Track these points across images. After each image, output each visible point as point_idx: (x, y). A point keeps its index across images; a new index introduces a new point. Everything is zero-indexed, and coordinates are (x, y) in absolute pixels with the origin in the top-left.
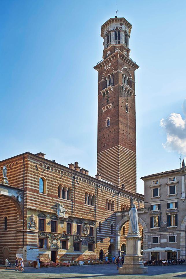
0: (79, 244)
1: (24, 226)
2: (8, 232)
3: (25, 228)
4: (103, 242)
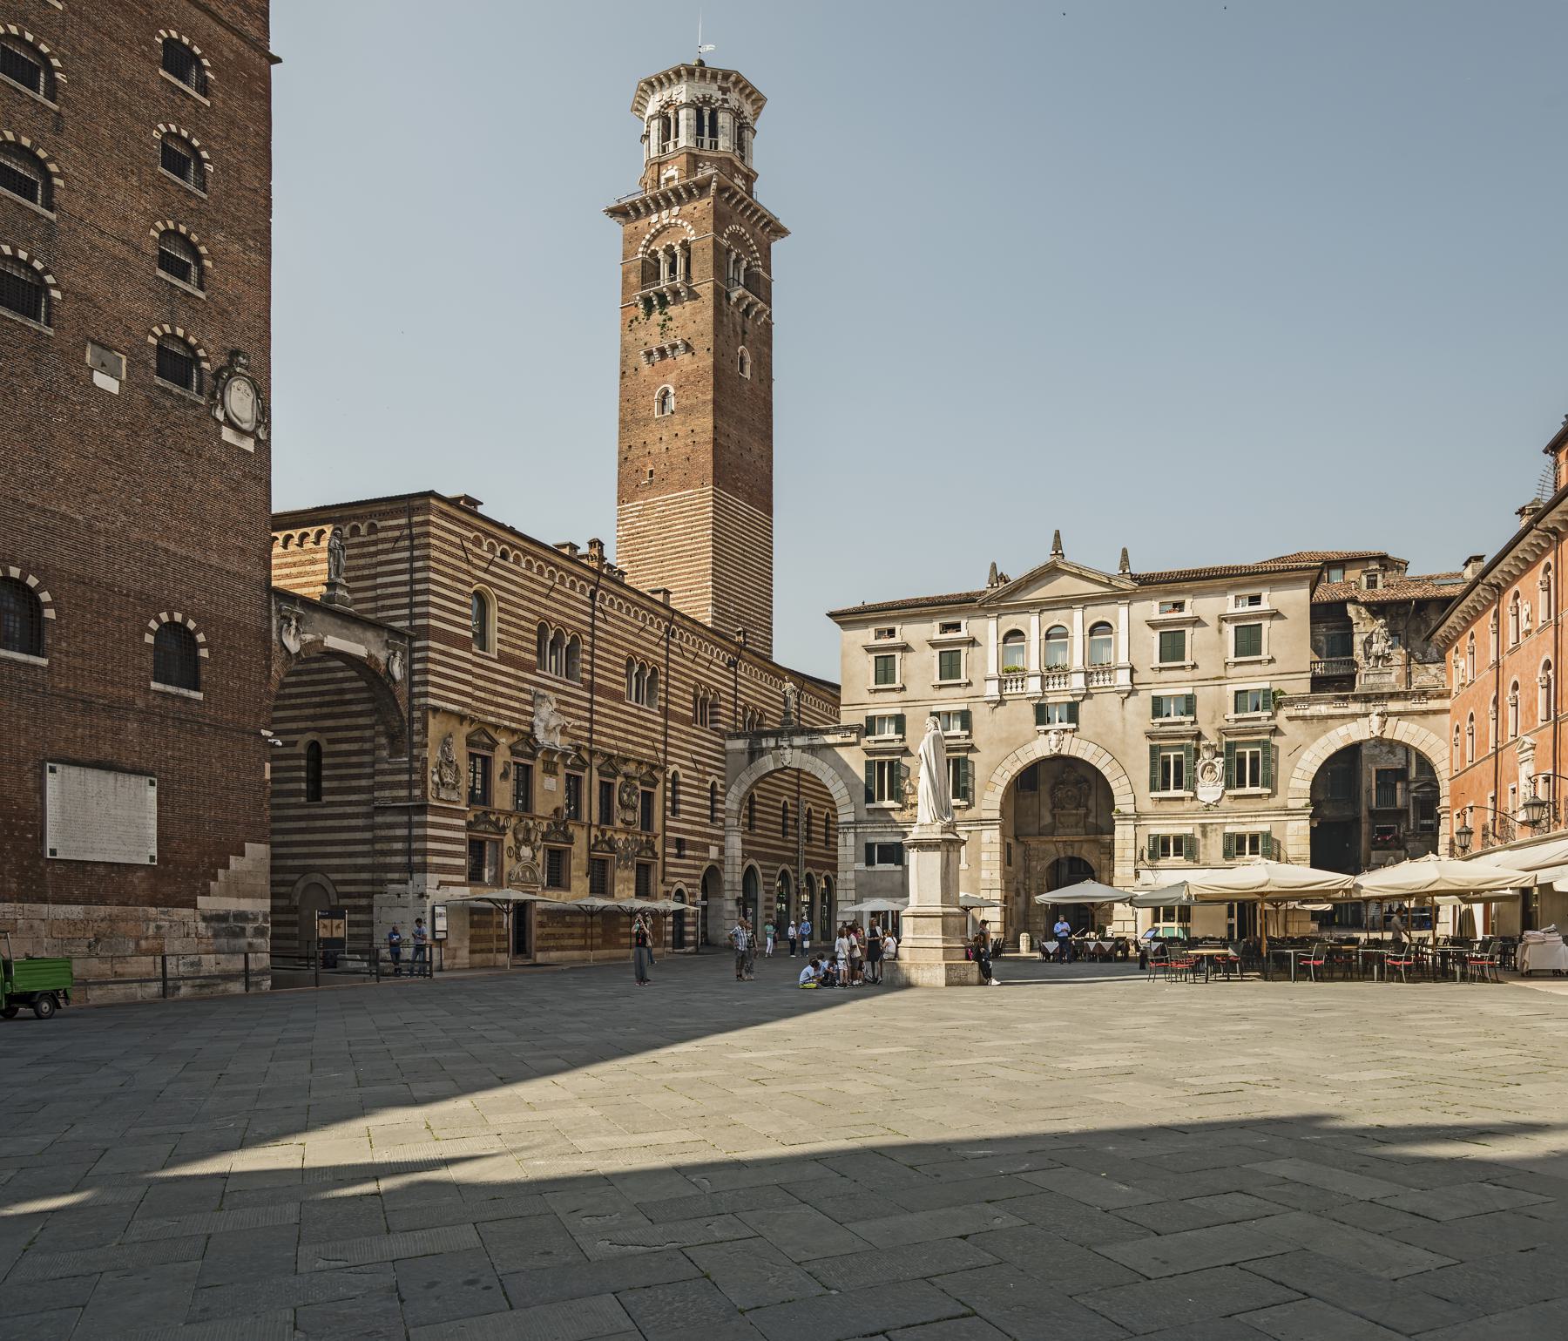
0: (603, 863)
1: (410, 785)
4: (684, 857)
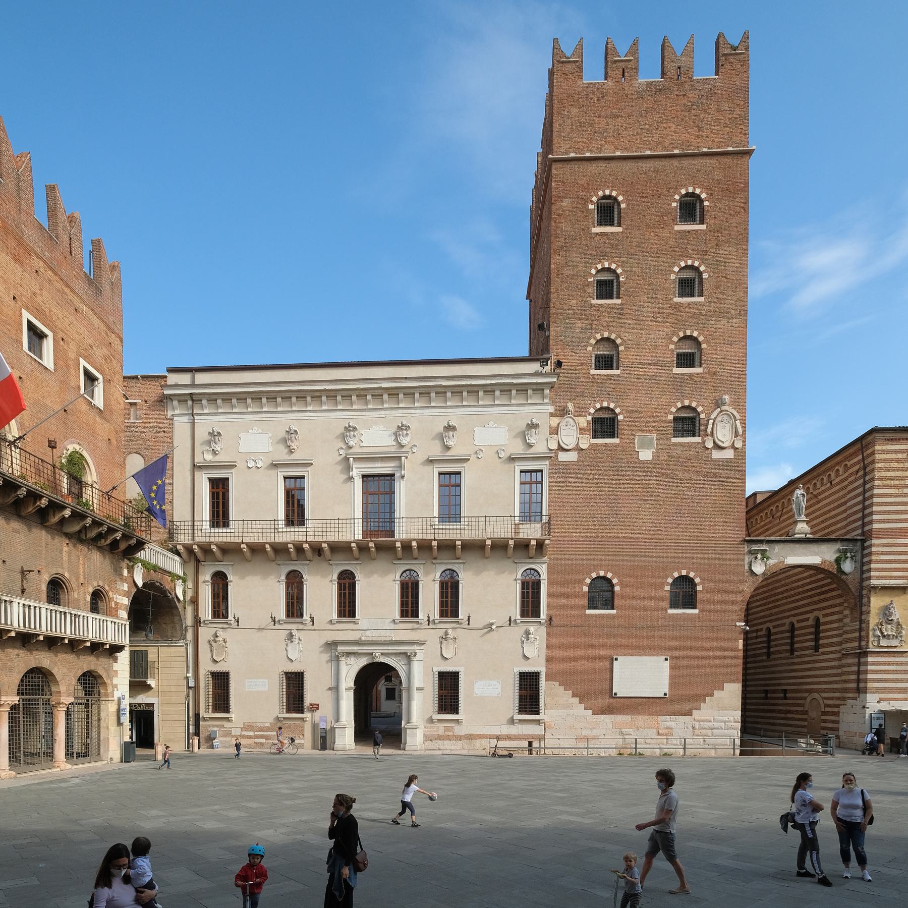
2: (821, 657)
3: (863, 643)
